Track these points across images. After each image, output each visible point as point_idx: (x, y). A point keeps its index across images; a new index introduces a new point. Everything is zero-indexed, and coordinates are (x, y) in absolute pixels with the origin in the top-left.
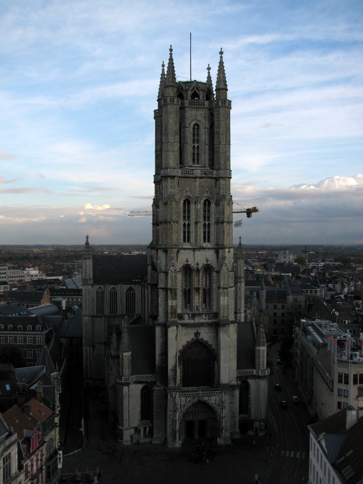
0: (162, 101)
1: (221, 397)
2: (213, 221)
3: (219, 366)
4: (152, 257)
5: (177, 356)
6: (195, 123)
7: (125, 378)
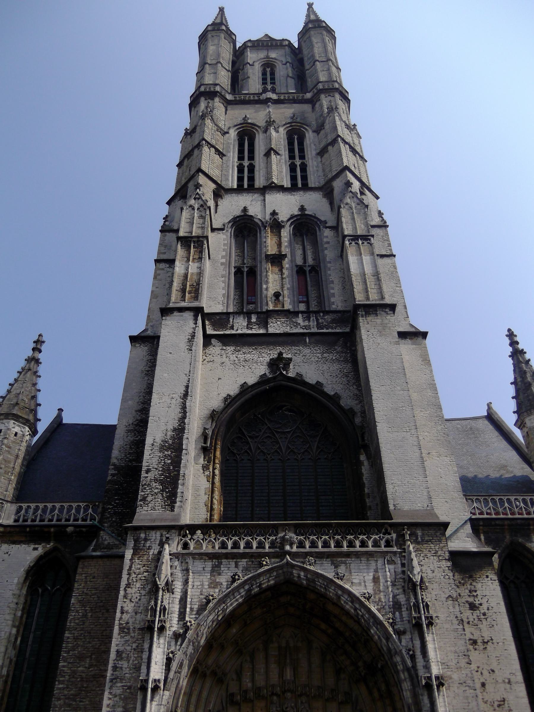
1: (403, 565)
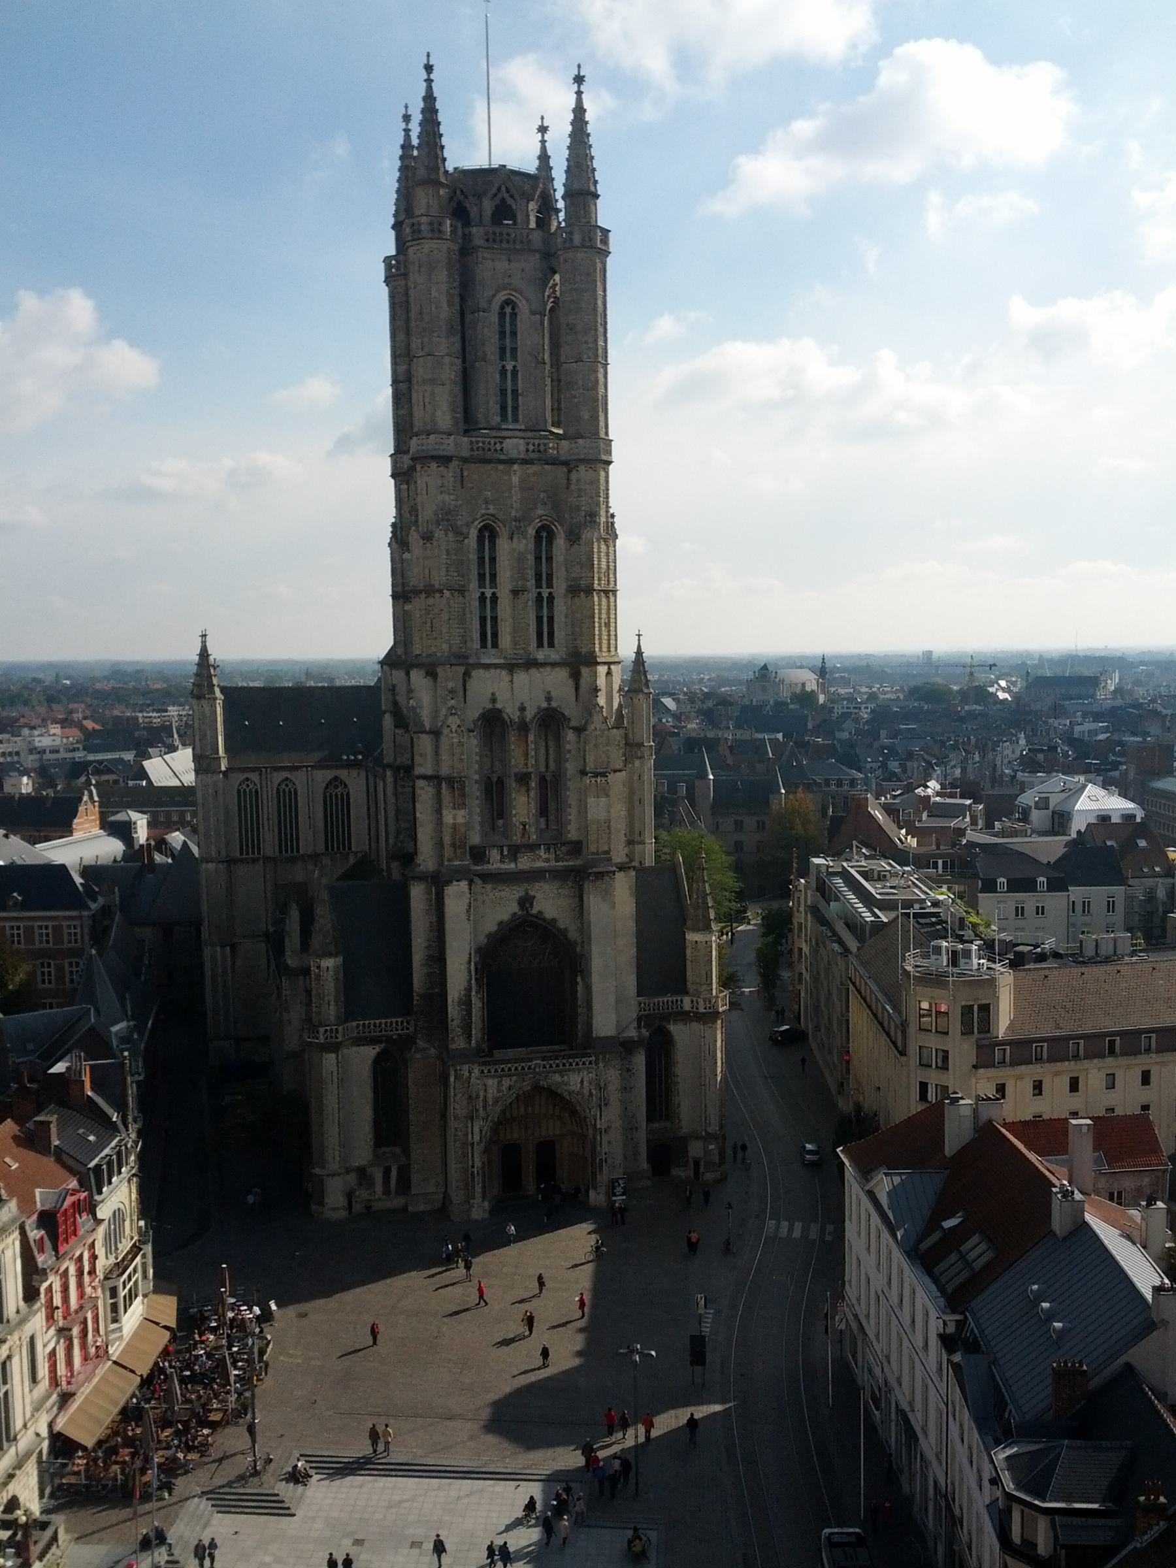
0: (408, 230)
2: (560, 586)
3: (588, 988)
4: (394, 690)
5: (472, 963)
6: (506, 297)
7: (326, 1030)
